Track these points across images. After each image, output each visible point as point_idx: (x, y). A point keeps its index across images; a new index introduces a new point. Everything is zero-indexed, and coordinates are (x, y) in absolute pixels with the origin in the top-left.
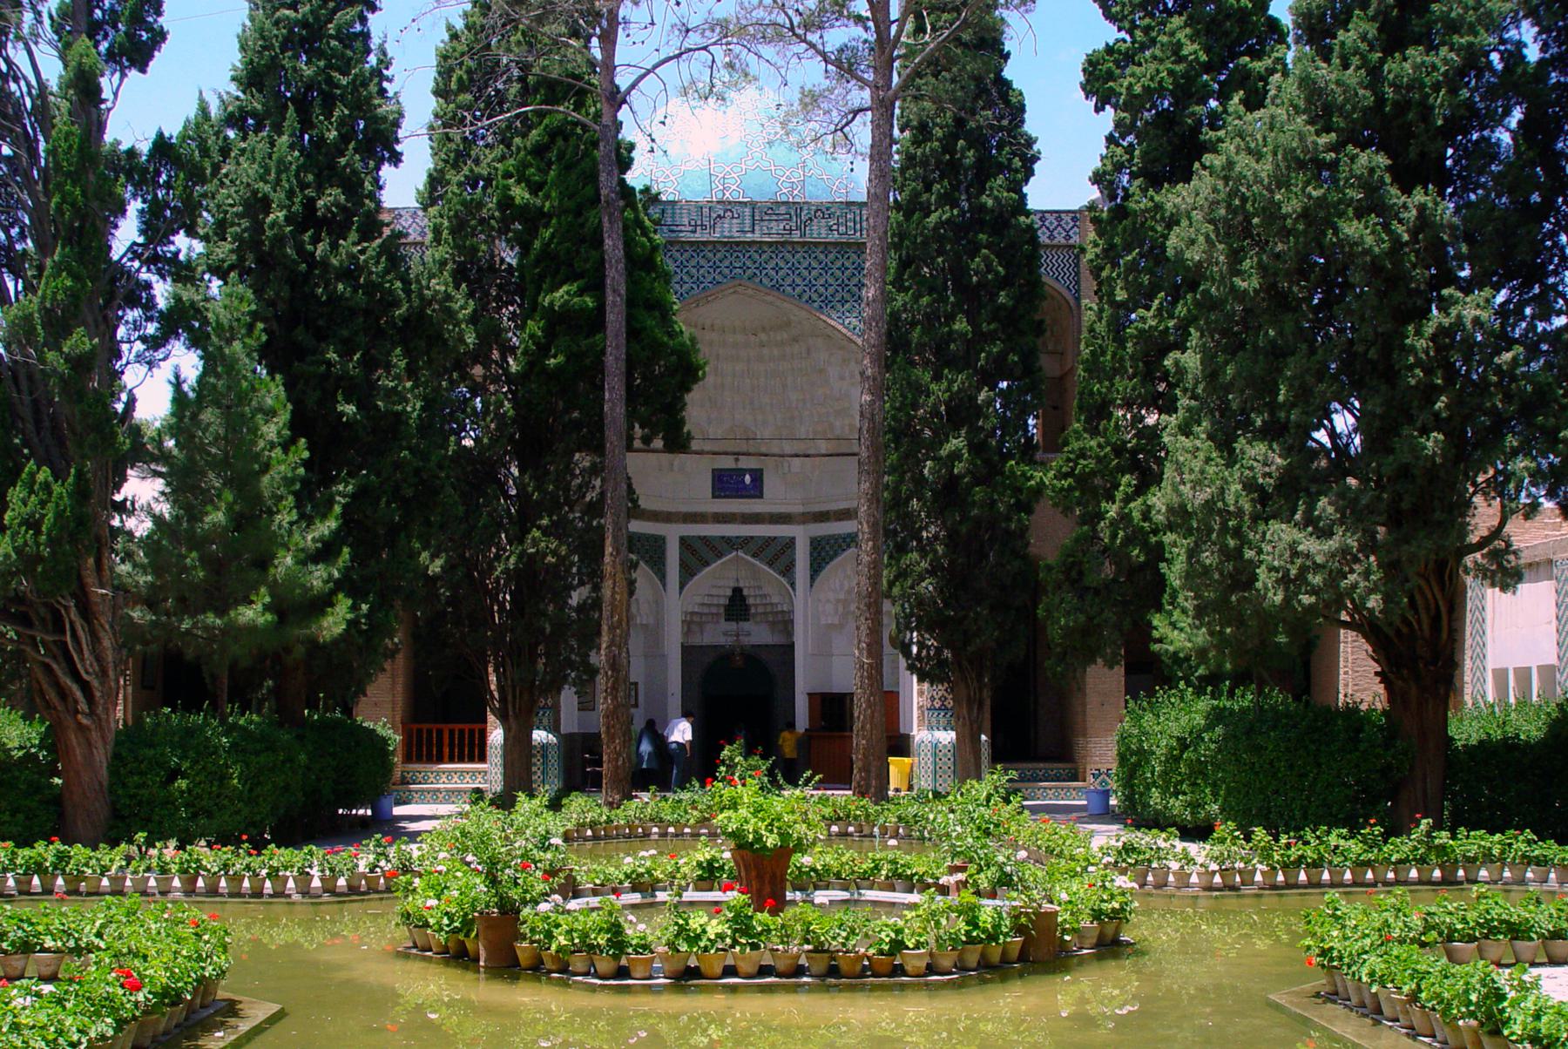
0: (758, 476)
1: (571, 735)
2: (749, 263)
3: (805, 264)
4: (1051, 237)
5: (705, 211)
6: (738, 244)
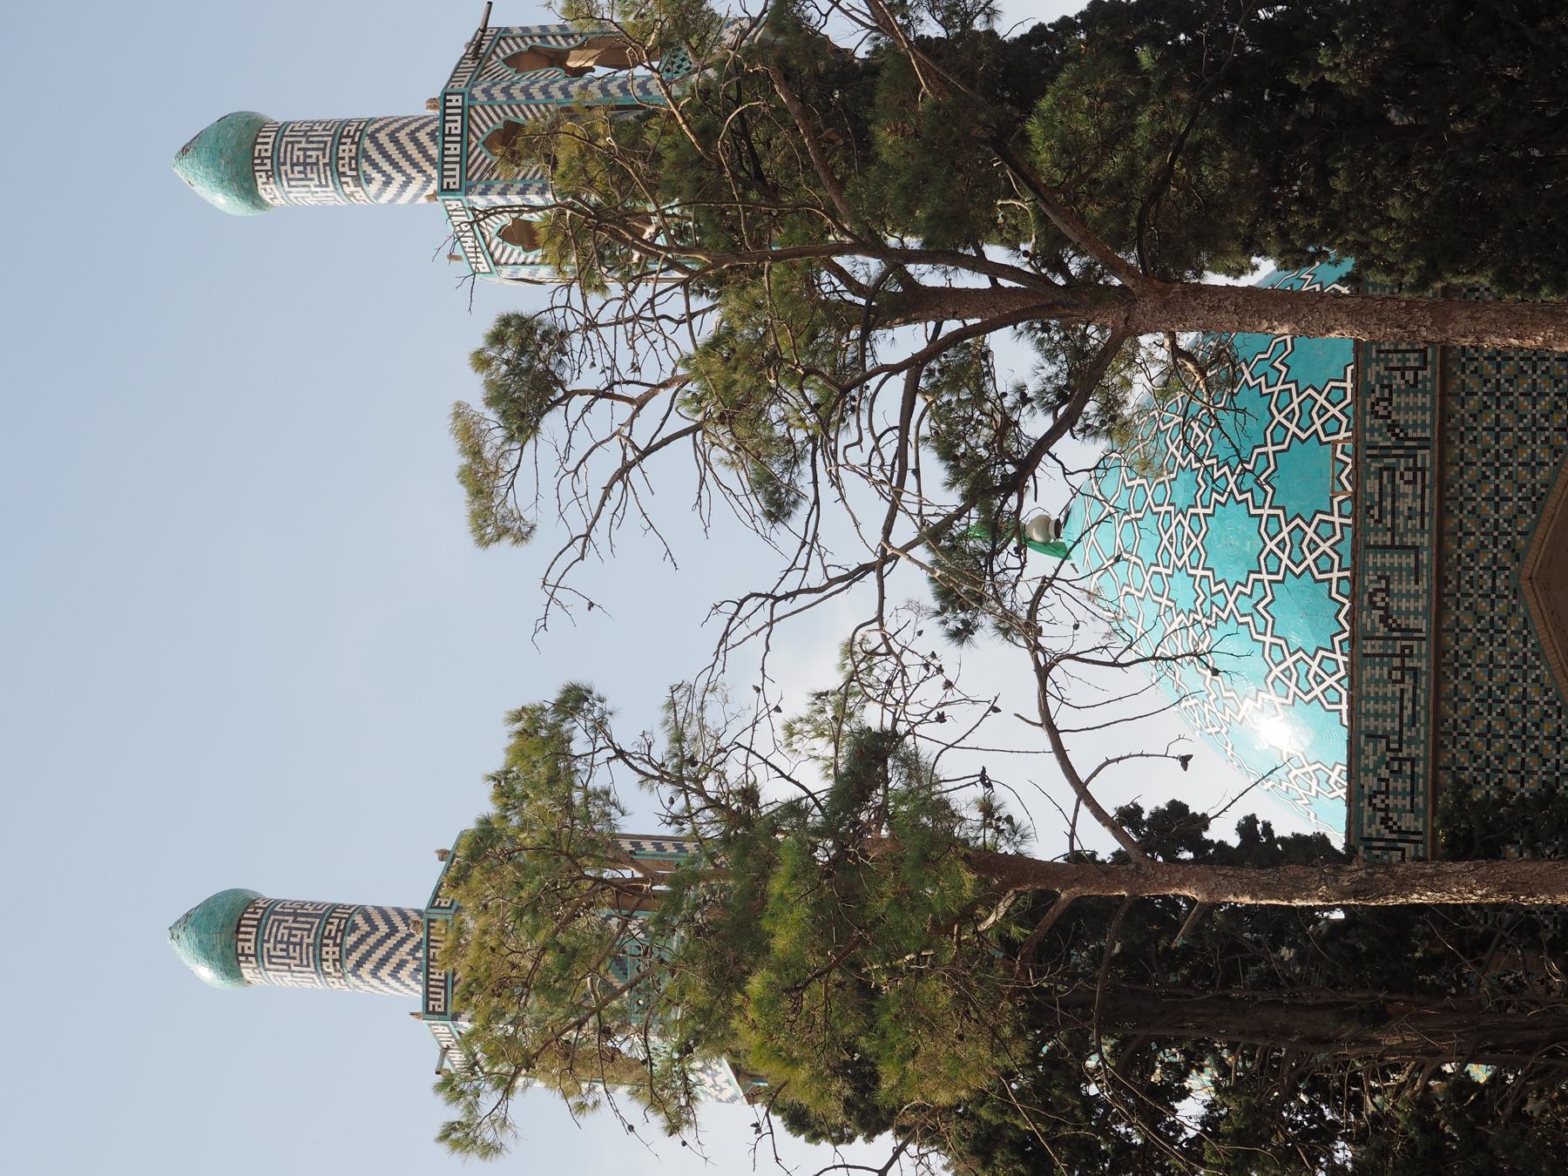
2: (1485, 560)
3: (1489, 438)
5: (1369, 647)
6: (1441, 581)
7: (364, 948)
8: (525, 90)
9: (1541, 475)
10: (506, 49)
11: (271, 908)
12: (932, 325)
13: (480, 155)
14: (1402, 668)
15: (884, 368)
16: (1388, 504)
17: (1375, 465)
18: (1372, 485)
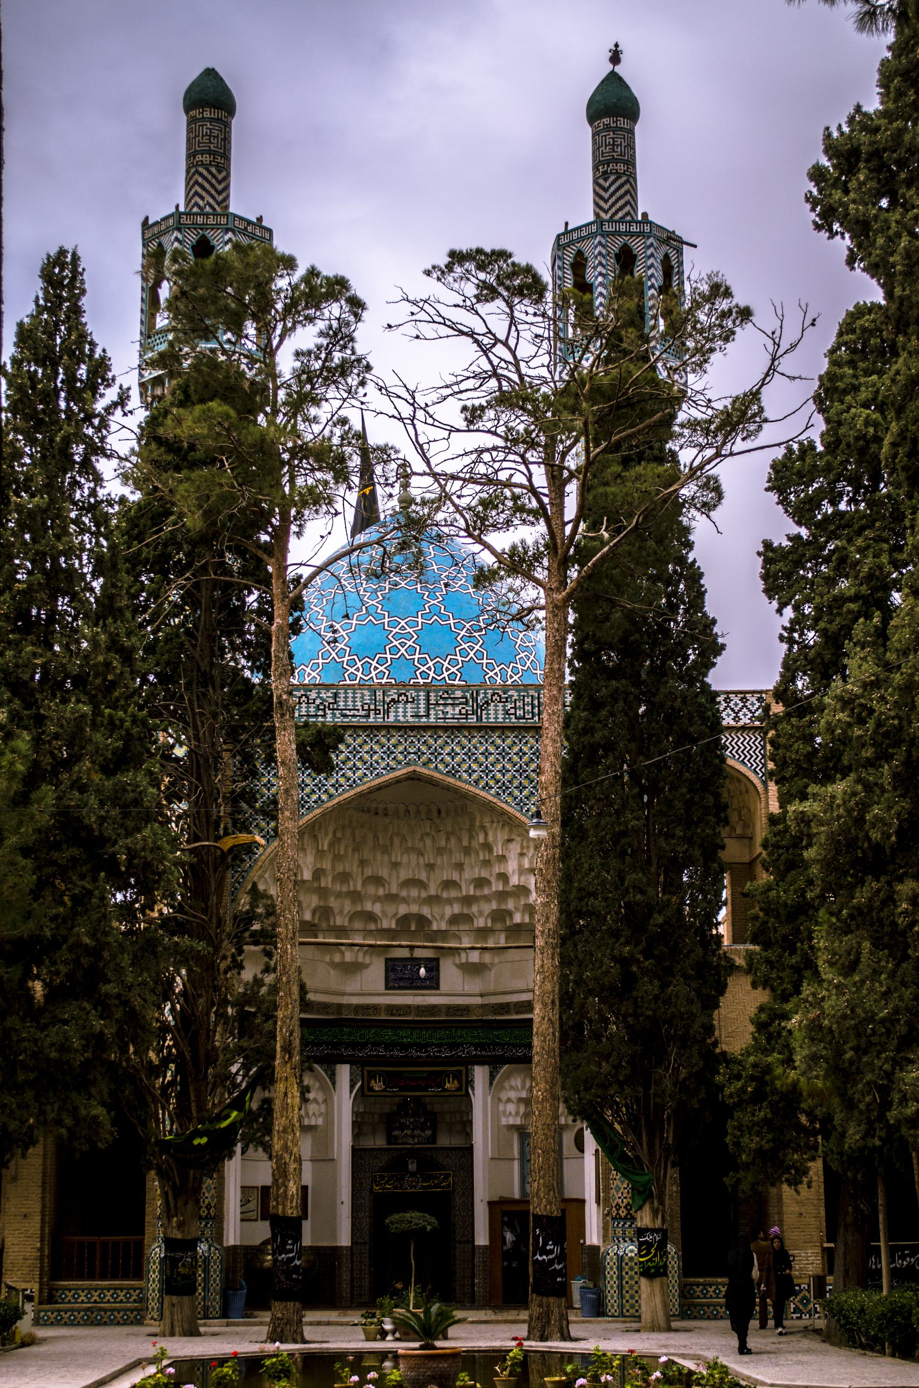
0: (433, 966)
1: (235, 1247)
2: (424, 749)
3: (482, 749)
4: (736, 719)
5: (379, 694)
6: (412, 728)
7: (209, 177)
8: (652, 265)
9: (465, 775)
10: (673, 254)
11: (227, 125)
12: (546, 491)
13: (620, 241)
14: (369, 710)
15: (531, 474)
16: (450, 701)
17: (468, 695)
18: (458, 694)
